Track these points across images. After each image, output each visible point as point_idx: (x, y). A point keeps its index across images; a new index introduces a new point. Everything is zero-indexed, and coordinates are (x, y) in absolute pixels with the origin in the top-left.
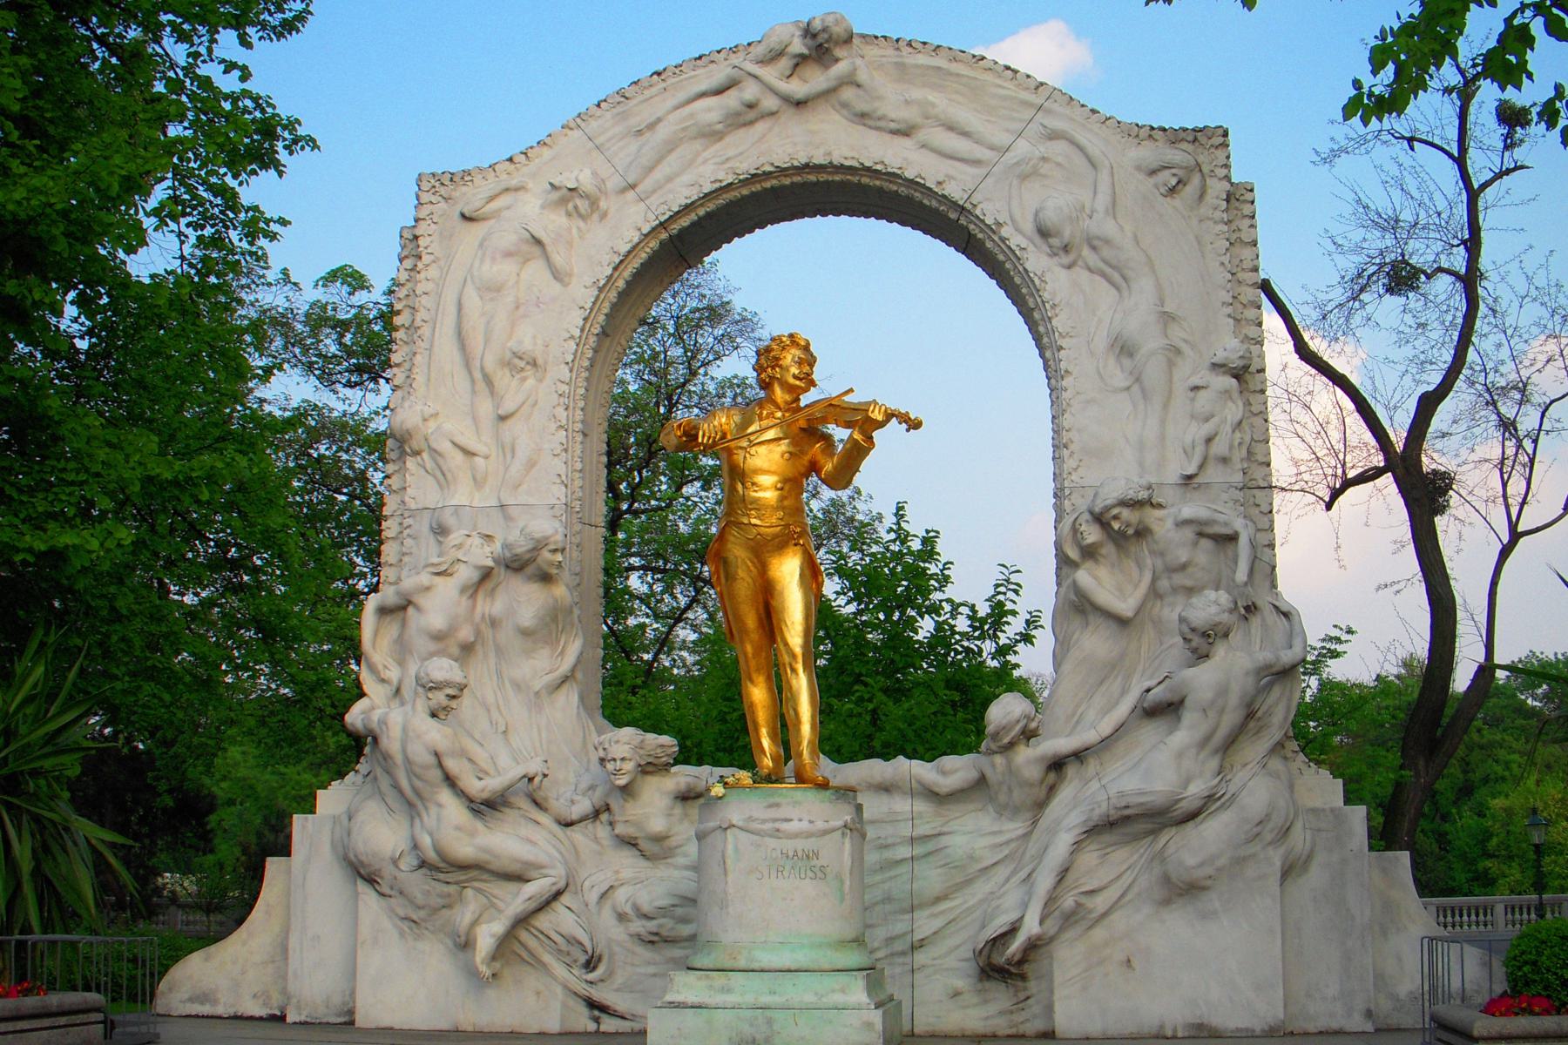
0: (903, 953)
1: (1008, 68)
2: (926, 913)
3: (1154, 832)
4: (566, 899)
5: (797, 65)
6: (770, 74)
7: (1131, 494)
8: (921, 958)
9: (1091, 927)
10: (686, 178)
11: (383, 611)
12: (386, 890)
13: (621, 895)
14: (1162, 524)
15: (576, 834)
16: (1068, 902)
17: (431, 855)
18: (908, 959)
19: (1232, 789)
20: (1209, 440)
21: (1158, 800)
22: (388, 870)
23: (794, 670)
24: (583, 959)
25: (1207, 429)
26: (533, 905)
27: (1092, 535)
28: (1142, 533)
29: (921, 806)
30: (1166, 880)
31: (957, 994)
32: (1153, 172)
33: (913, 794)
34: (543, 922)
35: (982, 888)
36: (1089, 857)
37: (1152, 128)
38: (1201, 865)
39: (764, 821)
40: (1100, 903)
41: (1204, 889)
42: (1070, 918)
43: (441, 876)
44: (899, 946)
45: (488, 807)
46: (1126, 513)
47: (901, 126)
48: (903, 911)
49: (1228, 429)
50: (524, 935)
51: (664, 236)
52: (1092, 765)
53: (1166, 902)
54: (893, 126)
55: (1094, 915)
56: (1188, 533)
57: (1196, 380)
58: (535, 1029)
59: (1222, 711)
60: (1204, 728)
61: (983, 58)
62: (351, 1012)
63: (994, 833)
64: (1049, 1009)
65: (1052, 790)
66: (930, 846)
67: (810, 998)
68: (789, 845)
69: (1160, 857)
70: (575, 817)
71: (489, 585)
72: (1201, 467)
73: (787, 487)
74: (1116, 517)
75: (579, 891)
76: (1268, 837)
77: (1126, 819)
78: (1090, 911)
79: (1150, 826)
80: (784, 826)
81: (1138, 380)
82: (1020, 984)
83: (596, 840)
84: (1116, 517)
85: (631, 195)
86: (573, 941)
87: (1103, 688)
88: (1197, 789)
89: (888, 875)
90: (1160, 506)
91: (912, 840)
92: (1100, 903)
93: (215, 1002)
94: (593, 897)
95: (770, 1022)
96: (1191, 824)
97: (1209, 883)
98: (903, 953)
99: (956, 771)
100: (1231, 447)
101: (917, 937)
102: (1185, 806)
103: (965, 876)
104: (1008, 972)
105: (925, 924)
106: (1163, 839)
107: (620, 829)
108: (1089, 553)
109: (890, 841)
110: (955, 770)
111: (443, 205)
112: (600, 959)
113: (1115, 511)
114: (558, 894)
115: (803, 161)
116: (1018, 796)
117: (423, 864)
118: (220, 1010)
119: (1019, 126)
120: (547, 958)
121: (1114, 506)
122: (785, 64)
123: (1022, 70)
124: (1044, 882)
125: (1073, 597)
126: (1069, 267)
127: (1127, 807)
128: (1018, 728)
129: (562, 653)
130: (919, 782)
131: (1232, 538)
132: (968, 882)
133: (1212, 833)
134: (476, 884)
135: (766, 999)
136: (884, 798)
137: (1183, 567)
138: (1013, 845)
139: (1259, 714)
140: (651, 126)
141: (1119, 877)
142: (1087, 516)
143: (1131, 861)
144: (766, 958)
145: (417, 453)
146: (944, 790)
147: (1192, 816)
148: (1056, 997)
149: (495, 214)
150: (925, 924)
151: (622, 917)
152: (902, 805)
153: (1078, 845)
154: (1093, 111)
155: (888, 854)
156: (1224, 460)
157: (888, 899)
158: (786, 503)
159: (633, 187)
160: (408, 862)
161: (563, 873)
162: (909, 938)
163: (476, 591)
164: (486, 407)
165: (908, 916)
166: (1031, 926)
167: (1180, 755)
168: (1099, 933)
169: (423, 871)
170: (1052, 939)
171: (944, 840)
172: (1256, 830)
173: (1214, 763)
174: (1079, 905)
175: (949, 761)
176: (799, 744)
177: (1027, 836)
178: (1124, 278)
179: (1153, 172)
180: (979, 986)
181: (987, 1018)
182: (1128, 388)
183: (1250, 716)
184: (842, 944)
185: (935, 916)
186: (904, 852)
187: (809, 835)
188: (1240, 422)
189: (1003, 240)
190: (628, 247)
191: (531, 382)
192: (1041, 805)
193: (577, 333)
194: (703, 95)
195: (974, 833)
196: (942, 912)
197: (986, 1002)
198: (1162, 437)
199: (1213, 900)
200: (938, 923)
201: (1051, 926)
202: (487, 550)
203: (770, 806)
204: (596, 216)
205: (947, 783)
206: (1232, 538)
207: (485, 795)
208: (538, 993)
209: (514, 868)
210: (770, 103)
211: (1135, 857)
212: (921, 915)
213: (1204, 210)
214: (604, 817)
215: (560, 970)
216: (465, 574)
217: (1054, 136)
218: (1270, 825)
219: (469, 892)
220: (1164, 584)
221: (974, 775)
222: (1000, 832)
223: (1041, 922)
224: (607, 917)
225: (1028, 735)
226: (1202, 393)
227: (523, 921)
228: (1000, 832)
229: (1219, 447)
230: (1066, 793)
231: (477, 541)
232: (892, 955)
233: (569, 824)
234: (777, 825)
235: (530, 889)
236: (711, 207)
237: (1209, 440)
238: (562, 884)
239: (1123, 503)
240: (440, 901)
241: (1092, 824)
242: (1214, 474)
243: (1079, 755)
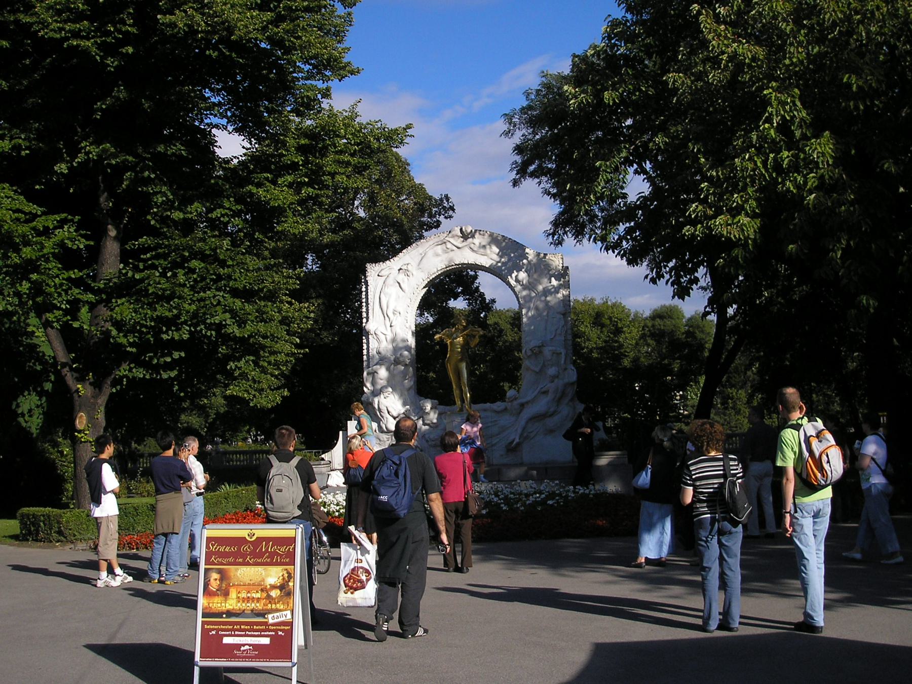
6: (452, 240)
14: (547, 351)
27: (529, 353)
28: (540, 352)
40: (532, 435)
65: (521, 411)
88: (552, 410)
92: (532, 435)
105: (495, 441)
108: (529, 357)
110: (498, 405)
124: (519, 431)
133: (556, 419)
150: (495, 441)
151: (427, 441)
153: (527, 423)
156: (560, 334)
164: (388, 324)
166: (517, 440)
175: (499, 403)
183: (563, 394)
205: (499, 409)
210: (455, 248)
225: (516, 399)
243: (527, 403)
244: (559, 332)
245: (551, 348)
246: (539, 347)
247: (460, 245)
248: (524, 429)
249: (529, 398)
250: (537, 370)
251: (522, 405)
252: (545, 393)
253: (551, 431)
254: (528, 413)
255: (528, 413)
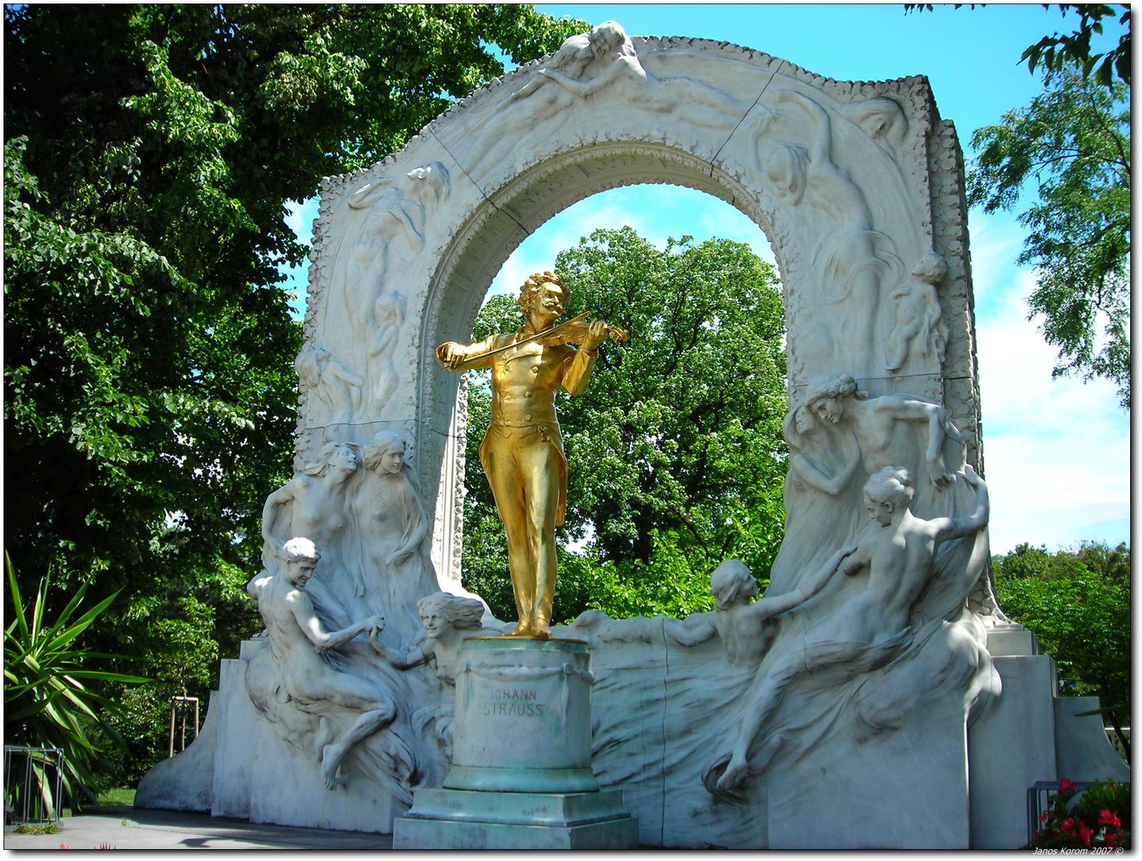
0: (656, 778)
1: (747, 49)
2: (677, 744)
3: (850, 678)
4: (395, 727)
5: (584, 67)
7: (832, 387)
8: (671, 782)
9: (798, 761)
10: (505, 164)
11: (278, 505)
12: (272, 717)
13: (439, 725)
15: (411, 677)
16: (775, 739)
17: (294, 694)
18: (660, 783)
19: (918, 638)
20: (909, 340)
21: (848, 651)
22: (272, 702)
23: (535, 543)
24: (407, 775)
25: (906, 330)
26: (365, 731)
27: (805, 423)
28: (846, 421)
29: (674, 655)
30: (860, 721)
31: (696, 814)
32: (864, 119)
33: (666, 645)
34: (375, 745)
35: (717, 725)
36: (796, 700)
37: (863, 84)
38: (890, 707)
39: (492, 667)
40: (808, 739)
41: (895, 729)
42: (781, 751)
43: (303, 707)
44: (654, 772)
45: (337, 655)
46: (829, 404)
47: (663, 105)
48: (658, 742)
49: (925, 327)
50: (362, 755)
51: (491, 210)
52: (799, 622)
53: (862, 741)
54: (657, 106)
55: (801, 750)
56: (885, 418)
57: (899, 291)
58: (373, 830)
59: (903, 570)
60: (887, 585)
61: (728, 43)
62: (247, 811)
63: (724, 678)
64: (765, 828)
65: (769, 642)
66: (679, 688)
67: (518, 816)
68: (511, 687)
69: (854, 700)
70: (409, 662)
71: (355, 482)
72: (905, 360)
73: (534, 395)
74: (822, 408)
75: (408, 720)
76: (953, 683)
77: (824, 667)
78: (797, 746)
79: (846, 673)
80: (507, 671)
81: (850, 293)
82: (745, 807)
83: (426, 681)
84: (822, 408)
85: (466, 179)
86: (396, 760)
87: (818, 555)
88: (881, 640)
89: (646, 712)
90: (862, 398)
91: (666, 684)
92: (808, 739)
93: (173, 798)
94: (418, 725)
95: (484, 834)
96: (880, 672)
97: (897, 724)
98: (656, 778)
99: (697, 626)
100: (929, 345)
101: (667, 763)
102: (871, 656)
103: (706, 712)
104: (732, 796)
105: (674, 754)
106: (857, 684)
107: (441, 672)
109: (648, 684)
111: (338, 199)
112: (422, 775)
113: (819, 404)
114: (385, 724)
115: (591, 141)
116: (740, 647)
117: (290, 699)
118: (176, 805)
119: (755, 95)
120: (379, 774)
121: (819, 398)
122: (575, 68)
123: (759, 48)
125: (794, 478)
126: (797, 203)
127: (820, 657)
128: (732, 589)
129: (409, 534)
130: (670, 636)
131: (924, 421)
132: (707, 719)
133: (901, 677)
134: (327, 714)
135: (487, 815)
136: (646, 648)
137: (885, 447)
138: (741, 688)
139: (945, 573)
140: (481, 127)
141: (821, 718)
142: (803, 409)
143: (833, 702)
144: (478, 783)
145: (315, 386)
146: (687, 642)
147: (880, 664)
148: (769, 820)
149: (372, 204)
152: (659, 653)
153: (782, 692)
154: (814, 76)
155: (646, 696)
157: (645, 732)
158: (533, 407)
159: (467, 173)
160: (283, 696)
161: (391, 706)
162: (660, 766)
163: (343, 491)
165: (662, 747)
166: (738, 760)
167: (865, 611)
168: (807, 765)
169: (293, 703)
170: (765, 771)
171: (689, 684)
172: (941, 676)
173: (899, 618)
174: (784, 743)
176: (465, 599)
177: (750, 680)
178: (840, 210)
179: (864, 119)
180: (715, 807)
181: (720, 836)
182: (842, 301)
184: (555, 770)
185: (681, 747)
186: (659, 693)
187: (528, 678)
188: (937, 323)
189: (744, 187)
190: (462, 220)
191: (393, 328)
192: (763, 653)
193: (426, 289)
194: (517, 98)
195: (711, 678)
196: (687, 745)
197: (720, 821)
198: (871, 339)
199: (901, 739)
200: (682, 754)
201: (761, 760)
202: (352, 456)
203: (497, 654)
204: (442, 198)
206: (924, 421)
207: (328, 645)
208: (375, 801)
209: (354, 701)
211: (836, 699)
212: (671, 746)
213: (907, 147)
214: (432, 663)
215: (389, 784)
216: (335, 475)
217: (784, 98)
218: (954, 673)
219: (323, 721)
220: (869, 464)
221: (708, 629)
222: (730, 677)
223: (749, 756)
224: (431, 742)
226: (904, 298)
227: (358, 744)
228: (730, 677)
229: (918, 345)
230: (778, 645)
231: (344, 449)
232: (648, 779)
233: (403, 667)
234: (501, 670)
235: (363, 718)
236: (524, 185)
237: (909, 340)
238: (390, 715)
239: (825, 396)
240: (307, 727)
241: (793, 671)
242: (914, 368)
243: (790, 611)
244: (918, 345)
245: (880, 401)
246: (838, 396)
247: (585, 87)
248: (769, 717)
249: (796, 595)
250: (832, 485)
251: (771, 622)
252: (858, 570)
253: (882, 729)
254: (791, 649)
255: (791, 649)
